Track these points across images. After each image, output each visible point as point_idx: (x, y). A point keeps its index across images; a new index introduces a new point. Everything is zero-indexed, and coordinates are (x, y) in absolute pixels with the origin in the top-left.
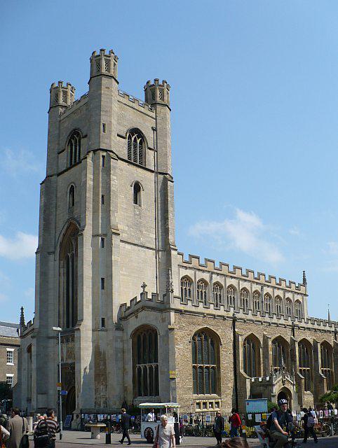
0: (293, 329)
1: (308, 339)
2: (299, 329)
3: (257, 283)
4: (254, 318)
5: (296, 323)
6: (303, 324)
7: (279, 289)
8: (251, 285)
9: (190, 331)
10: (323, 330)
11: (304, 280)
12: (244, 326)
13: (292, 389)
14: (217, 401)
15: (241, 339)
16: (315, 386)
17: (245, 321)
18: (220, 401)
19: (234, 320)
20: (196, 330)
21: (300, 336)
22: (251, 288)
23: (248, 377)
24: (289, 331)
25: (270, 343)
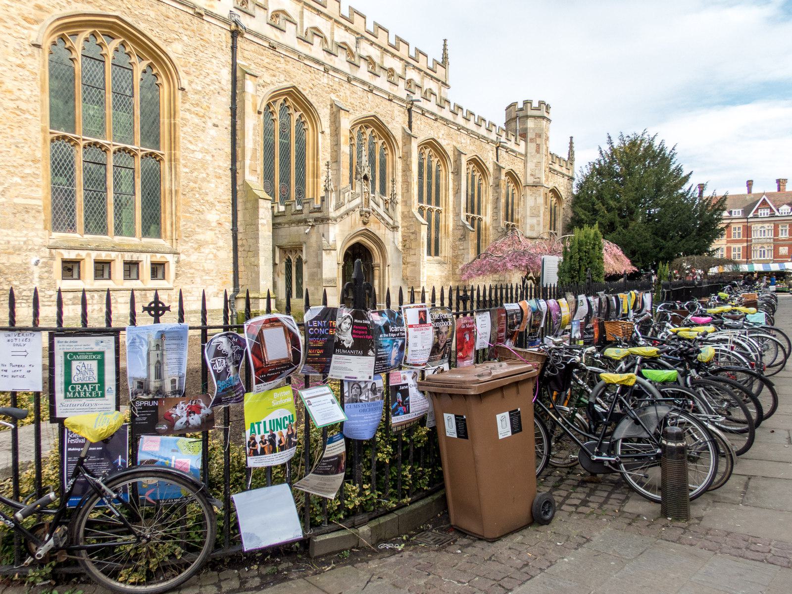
0: (409, 111)
1: (443, 142)
2: (423, 114)
3: (347, 29)
4: (303, 48)
5: (418, 95)
6: (431, 106)
7: (394, 55)
8: (332, 29)
9: (40, 8)
10: (473, 132)
11: (445, 57)
12: (267, 57)
13: (392, 240)
14: (158, 258)
15: (250, 85)
16: (454, 248)
17: (274, 48)
18: (170, 258)
19: (235, 34)
20: (68, 11)
21: (424, 130)
22: (332, 34)
23: (263, 194)
24: (402, 119)
25: (346, 123)
